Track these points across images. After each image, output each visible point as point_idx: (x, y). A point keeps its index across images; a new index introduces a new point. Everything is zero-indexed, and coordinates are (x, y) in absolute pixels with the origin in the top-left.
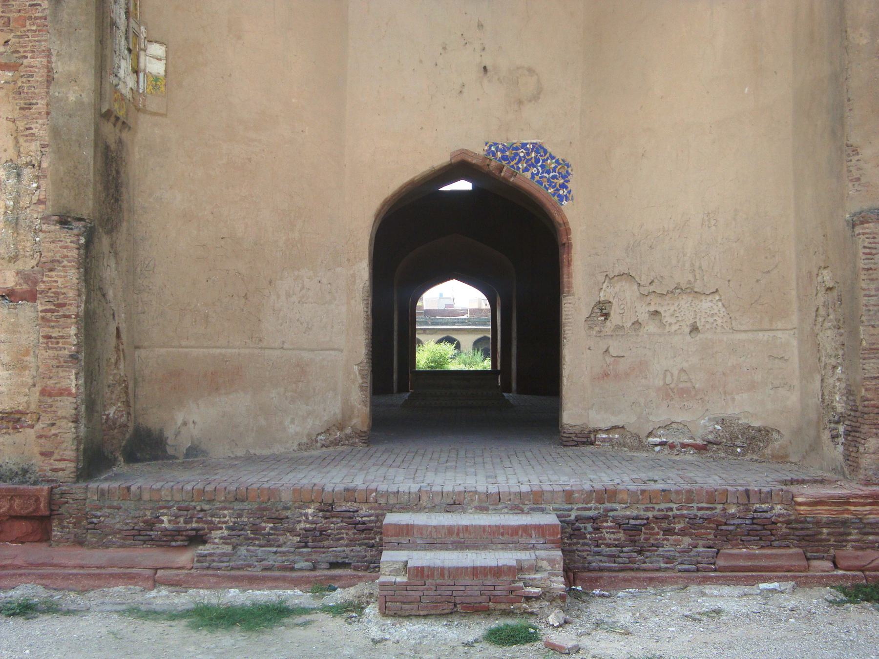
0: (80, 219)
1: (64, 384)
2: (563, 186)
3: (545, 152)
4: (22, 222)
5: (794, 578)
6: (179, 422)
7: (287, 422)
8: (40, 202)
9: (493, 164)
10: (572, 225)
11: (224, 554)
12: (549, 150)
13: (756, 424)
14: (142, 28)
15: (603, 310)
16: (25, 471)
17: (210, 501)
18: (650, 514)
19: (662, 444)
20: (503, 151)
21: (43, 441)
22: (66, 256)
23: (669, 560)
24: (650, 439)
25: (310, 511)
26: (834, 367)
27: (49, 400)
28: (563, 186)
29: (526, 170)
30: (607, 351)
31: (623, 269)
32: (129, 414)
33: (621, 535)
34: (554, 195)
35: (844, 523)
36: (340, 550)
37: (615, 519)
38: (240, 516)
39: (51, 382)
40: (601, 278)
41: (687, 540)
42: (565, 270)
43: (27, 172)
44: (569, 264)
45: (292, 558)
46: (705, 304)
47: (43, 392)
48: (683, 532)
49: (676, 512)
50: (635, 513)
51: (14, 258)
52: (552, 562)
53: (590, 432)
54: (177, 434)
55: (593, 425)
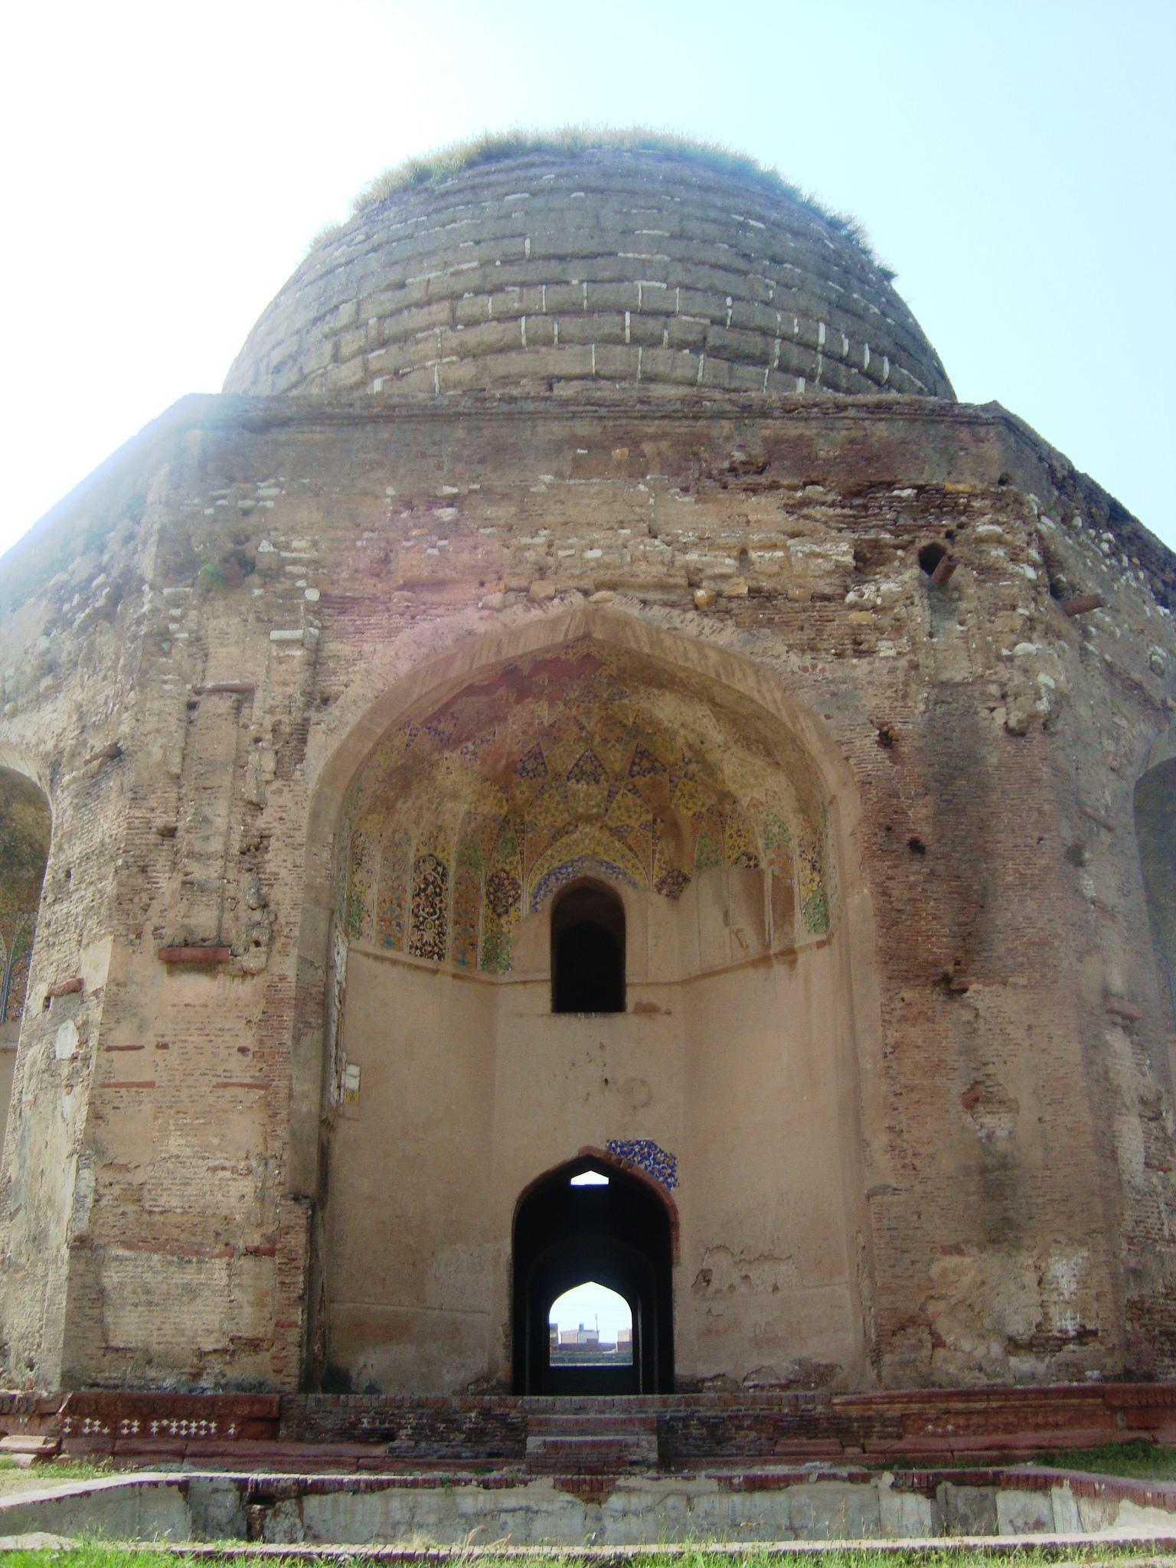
0: (306, 1197)
1: (293, 1318)
2: (671, 1175)
3: (656, 1147)
4: (266, 1198)
5: (831, 1460)
6: (361, 1364)
7: (444, 1371)
8: (280, 1184)
9: (614, 1158)
10: (679, 1207)
11: (409, 1447)
12: (659, 1145)
13: (824, 1362)
14: (344, 1054)
15: (705, 1277)
16: (261, 1384)
17: (399, 1407)
18: (725, 1415)
19: (755, 1386)
20: (621, 1147)
21: (275, 1361)
22: (297, 1224)
23: (740, 1448)
24: (746, 1384)
25: (473, 1415)
26: (870, 1308)
27: (282, 1330)
28: (671, 1175)
29: (640, 1162)
30: (709, 1311)
31: (718, 1242)
32: (324, 1354)
33: (704, 1431)
34: (663, 1182)
35: (869, 1418)
36: (496, 1444)
37: (699, 1419)
38: (421, 1418)
39: (283, 1317)
40: (703, 1251)
41: (753, 1435)
42: (674, 1245)
43: (272, 1163)
44: (677, 1241)
45: (459, 1449)
46: (783, 1268)
47: (277, 1325)
48: (750, 1428)
49: (743, 1412)
50: (714, 1414)
51: (260, 1225)
52: (649, 1442)
53: (698, 1381)
54: (359, 1374)
55: (700, 1376)
